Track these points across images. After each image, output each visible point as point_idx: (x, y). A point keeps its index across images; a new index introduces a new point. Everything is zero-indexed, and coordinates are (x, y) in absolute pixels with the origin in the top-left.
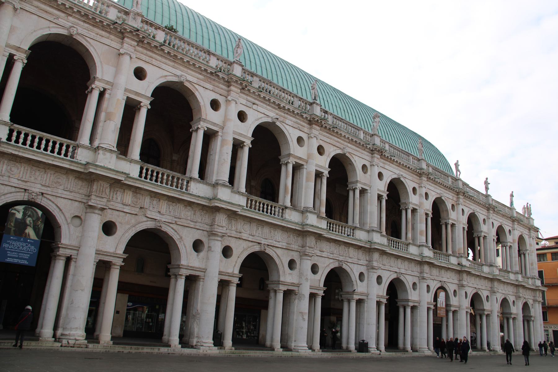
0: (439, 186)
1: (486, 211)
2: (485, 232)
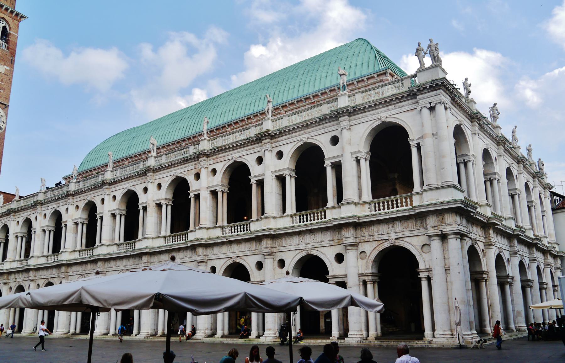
0: (174, 167)
1: (260, 144)
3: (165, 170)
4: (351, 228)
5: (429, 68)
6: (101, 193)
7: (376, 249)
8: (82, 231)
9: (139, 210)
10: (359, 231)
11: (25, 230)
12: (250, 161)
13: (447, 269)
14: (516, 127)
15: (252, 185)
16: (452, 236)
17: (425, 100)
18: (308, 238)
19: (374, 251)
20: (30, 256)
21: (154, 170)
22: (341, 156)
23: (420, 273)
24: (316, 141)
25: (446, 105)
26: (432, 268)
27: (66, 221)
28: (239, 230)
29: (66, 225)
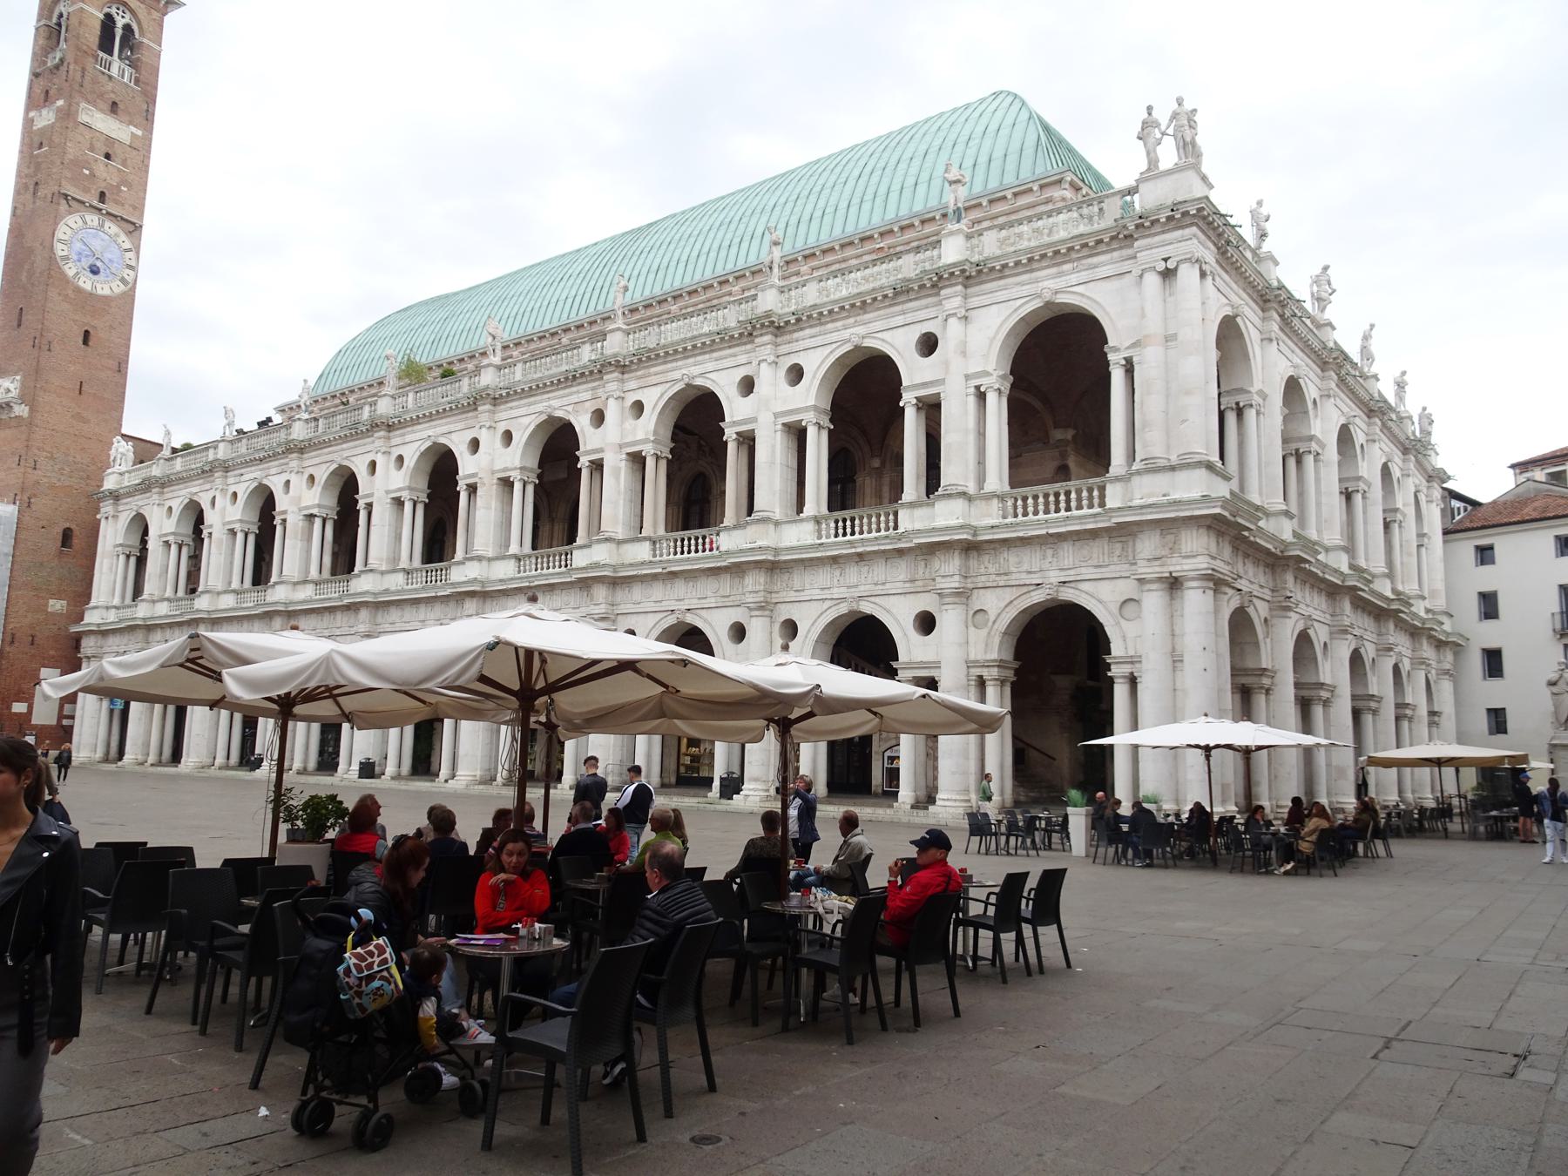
0: (544, 393)
1: (749, 347)
2: (734, 423)
3: (521, 398)
4: (957, 553)
5: (1169, 172)
6: (368, 448)
7: (1012, 605)
8: (321, 538)
9: (459, 492)
10: (973, 563)
11: (188, 529)
12: (725, 387)
13: (1176, 661)
14: (1372, 326)
15: (726, 442)
16: (1194, 584)
17: (1152, 251)
18: (853, 574)
19: (1007, 610)
20: (200, 590)
21: (495, 399)
22: (941, 382)
23: (1112, 667)
24: (884, 344)
25: (1204, 267)
26: (1140, 656)
27: (284, 512)
28: (693, 548)
29: (284, 521)
